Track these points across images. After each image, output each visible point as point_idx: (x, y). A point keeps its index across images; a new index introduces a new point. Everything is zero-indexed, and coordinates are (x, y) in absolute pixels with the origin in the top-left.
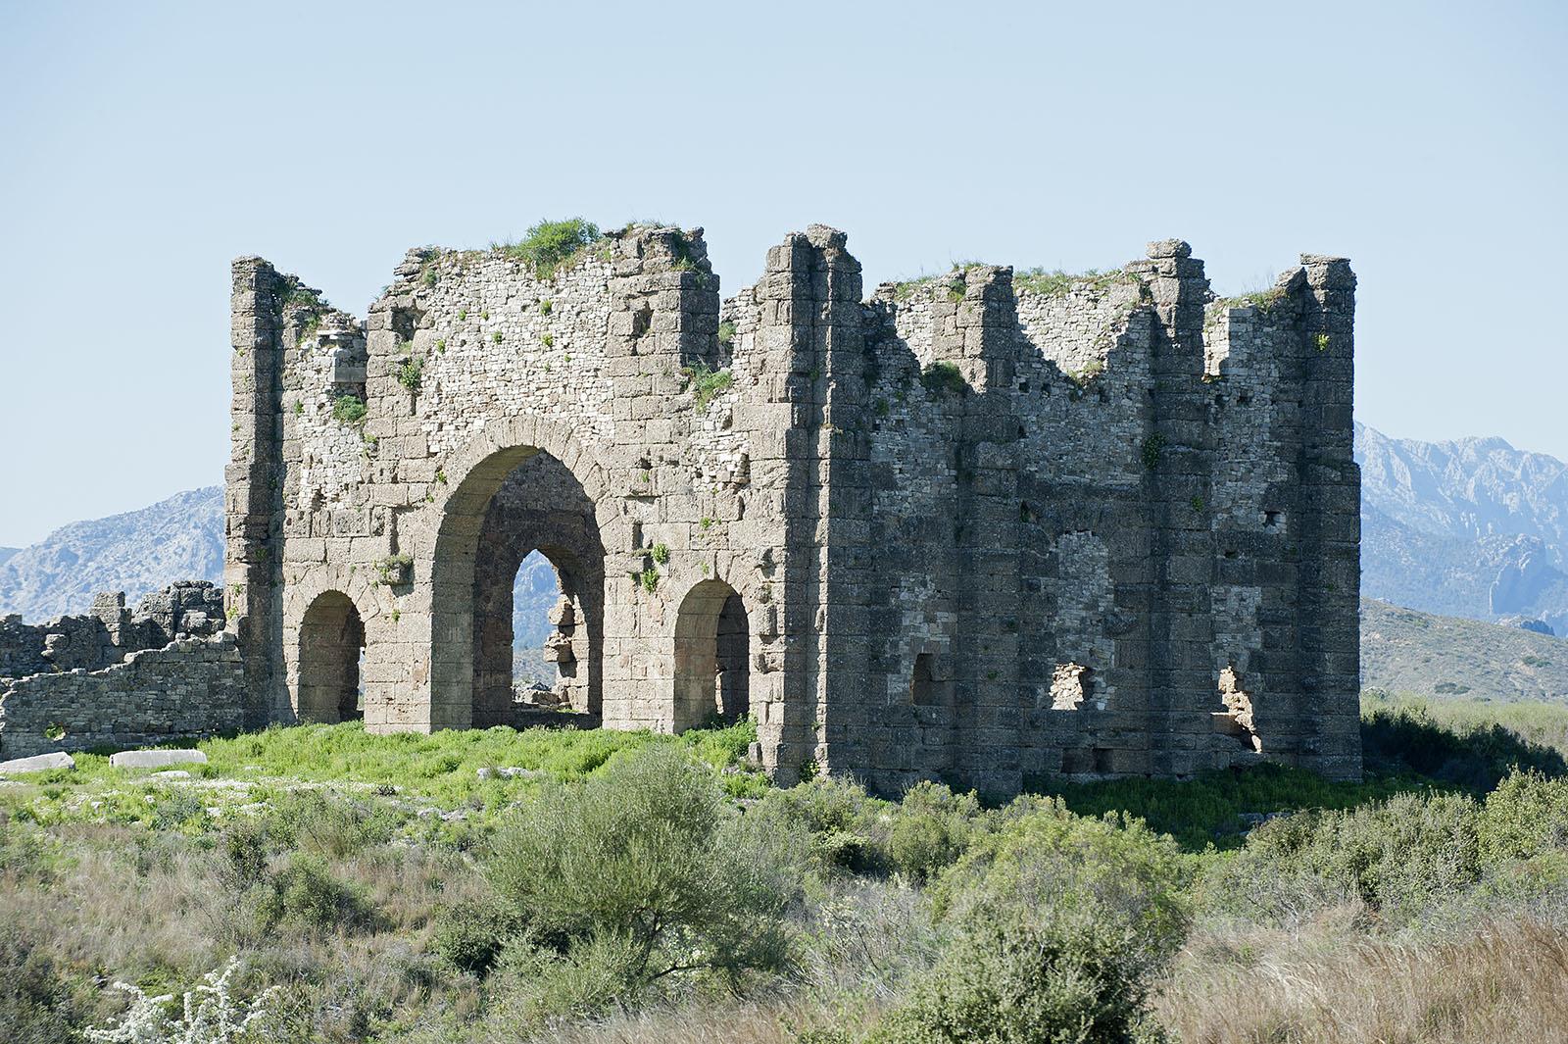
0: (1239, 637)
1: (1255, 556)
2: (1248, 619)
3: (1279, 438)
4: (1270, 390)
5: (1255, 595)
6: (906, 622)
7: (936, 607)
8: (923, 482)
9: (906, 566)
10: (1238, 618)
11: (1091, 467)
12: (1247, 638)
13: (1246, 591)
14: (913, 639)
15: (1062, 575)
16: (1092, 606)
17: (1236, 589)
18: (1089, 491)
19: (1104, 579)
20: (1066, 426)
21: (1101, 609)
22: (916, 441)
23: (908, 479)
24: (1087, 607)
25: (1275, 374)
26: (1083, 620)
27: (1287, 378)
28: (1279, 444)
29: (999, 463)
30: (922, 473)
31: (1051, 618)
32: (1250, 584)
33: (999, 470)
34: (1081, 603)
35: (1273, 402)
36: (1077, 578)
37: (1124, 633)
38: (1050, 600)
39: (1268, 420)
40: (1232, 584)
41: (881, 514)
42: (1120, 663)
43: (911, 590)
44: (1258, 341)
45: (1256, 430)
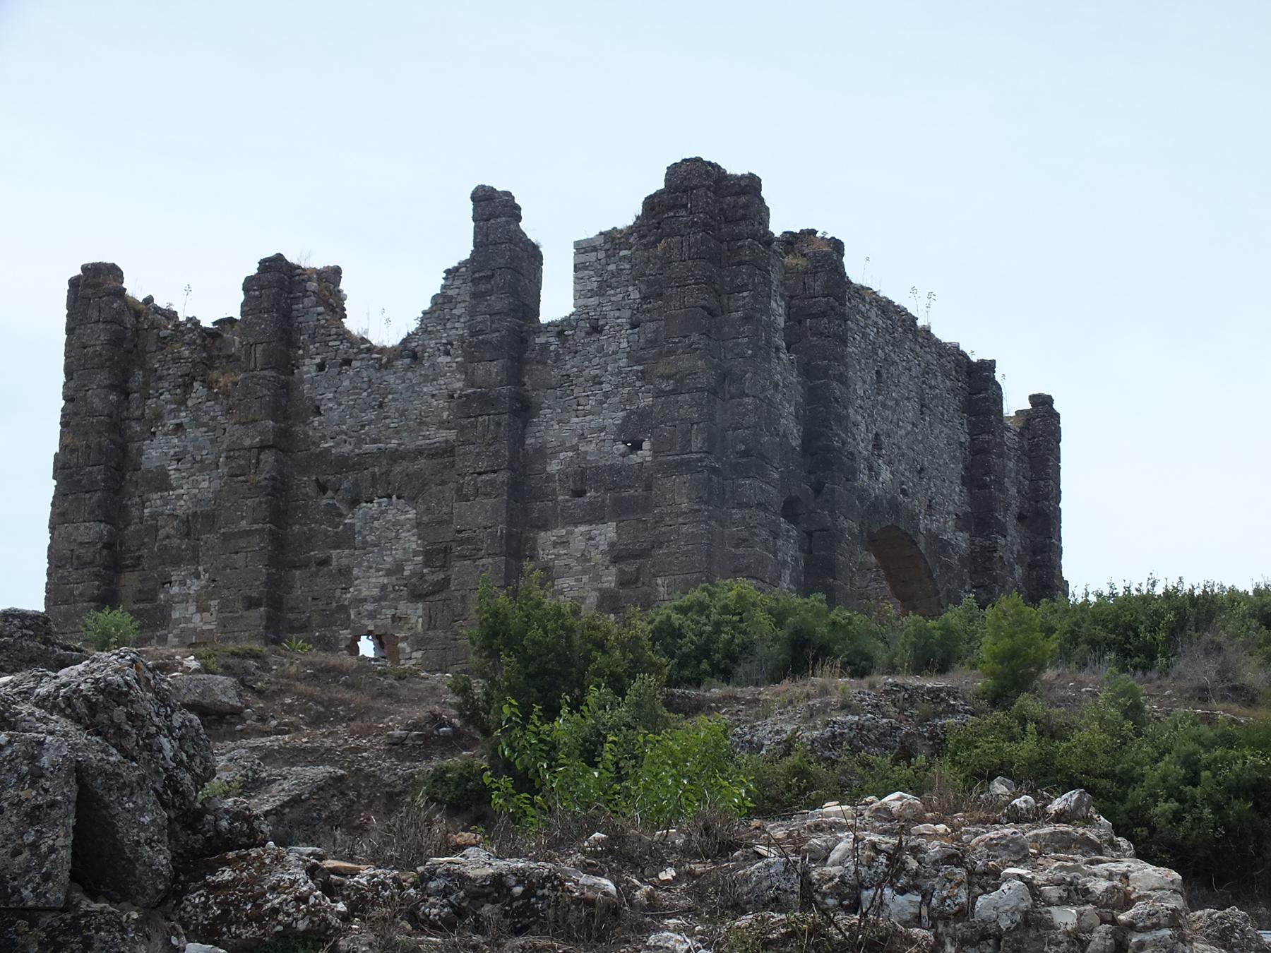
0: (585, 579)
1: (607, 490)
2: (597, 557)
3: (639, 361)
4: (627, 313)
5: (607, 532)
6: (175, 615)
8: (200, 478)
9: (176, 563)
10: (584, 558)
11: (398, 432)
12: (597, 578)
13: (595, 530)
14: (183, 630)
15: (358, 544)
16: (397, 569)
17: (582, 528)
18: (396, 456)
19: (411, 541)
20: (369, 395)
21: (406, 573)
22: (196, 439)
23: (184, 478)
24: (389, 573)
25: (635, 295)
26: (383, 587)
27: (648, 297)
28: (641, 368)
29: (247, 443)
30: (201, 471)
31: (345, 590)
32: (602, 520)
33: (249, 449)
34: (381, 570)
35: (633, 326)
36: (376, 546)
37: (433, 593)
38: (345, 574)
39: (625, 345)
40: (576, 525)
41: (153, 516)
42: (430, 624)
43: (183, 583)
44: (612, 267)
45: (609, 359)
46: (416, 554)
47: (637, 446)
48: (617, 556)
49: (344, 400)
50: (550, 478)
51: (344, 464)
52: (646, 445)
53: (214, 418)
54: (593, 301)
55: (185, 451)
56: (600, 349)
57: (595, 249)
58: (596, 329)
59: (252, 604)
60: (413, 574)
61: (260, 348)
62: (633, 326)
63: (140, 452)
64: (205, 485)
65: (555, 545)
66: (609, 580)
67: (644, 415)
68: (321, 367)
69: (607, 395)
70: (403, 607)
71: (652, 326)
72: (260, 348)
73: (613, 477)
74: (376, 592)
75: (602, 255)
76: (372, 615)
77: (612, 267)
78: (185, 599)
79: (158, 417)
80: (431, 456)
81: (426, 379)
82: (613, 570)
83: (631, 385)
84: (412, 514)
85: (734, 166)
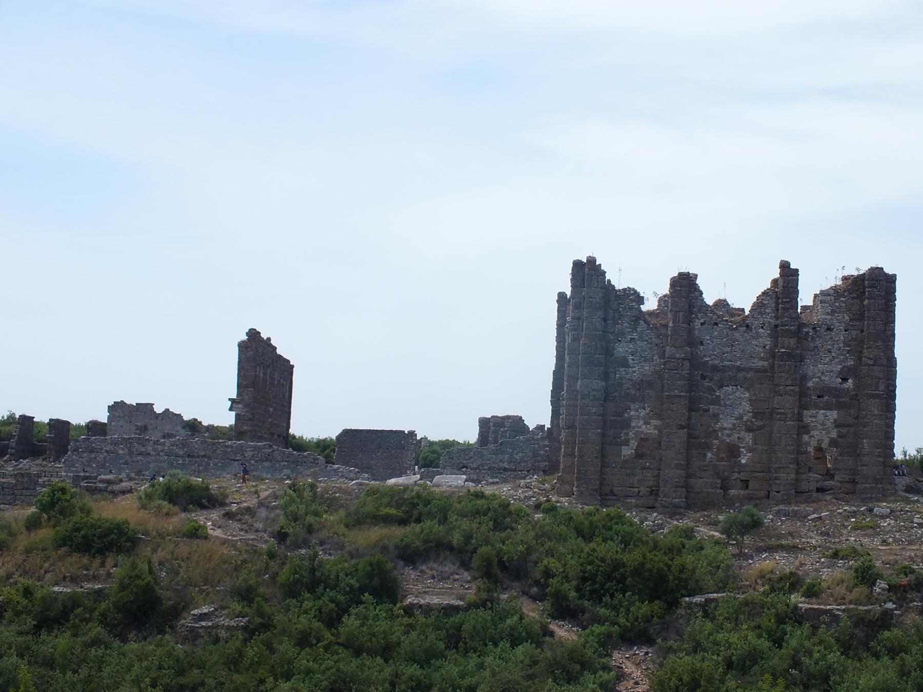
0: (824, 432)
2: (828, 424)
4: (844, 325)
5: (833, 415)
6: (633, 424)
7: (651, 418)
9: (634, 401)
10: (823, 424)
12: (829, 433)
13: (828, 413)
16: (740, 417)
17: (822, 411)
18: (739, 369)
24: (736, 419)
25: (847, 318)
26: (734, 424)
29: (678, 356)
38: (716, 416)
41: (620, 378)
42: (755, 443)
43: (637, 410)
44: (837, 304)
46: (749, 412)
47: (845, 380)
48: (837, 424)
49: (715, 340)
50: (809, 388)
51: (715, 369)
52: (850, 381)
53: (651, 338)
54: (829, 317)
55: (636, 351)
56: (831, 338)
57: (829, 295)
59: (682, 427)
60: (748, 420)
61: (681, 314)
64: (647, 368)
65: (811, 417)
66: (834, 434)
67: (849, 368)
68: (702, 324)
70: (743, 434)
71: (854, 332)
72: (681, 314)
74: (730, 426)
75: (833, 298)
76: (729, 436)
77: (837, 304)
78: (638, 418)
79: (623, 334)
81: (753, 338)
82: (835, 430)
83: (845, 355)
84: (747, 395)
85: (888, 270)
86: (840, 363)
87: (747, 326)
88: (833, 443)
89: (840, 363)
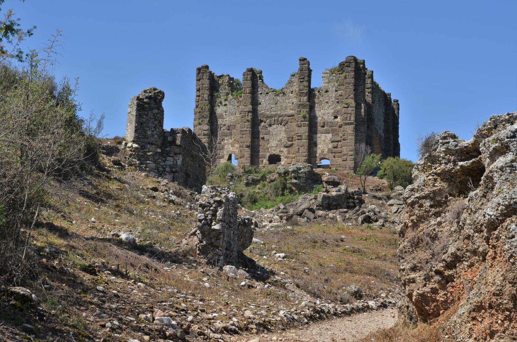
3: (337, 99)
4: (334, 88)
5: (330, 136)
6: (226, 147)
9: (226, 136)
13: (327, 135)
16: (281, 141)
24: (278, 141)
26: (277, 144)
29: (245, 110)
38: (268, 140)
43: (227, 140)
47: (336, 117)
51: (268, 117)
52: (339, 117)
54: (327, 85)
58: (327, 91)
62: (336, 91)
63: (216, 110)
66: (331, 146)
69: (330, 106)
73: (332, 125)
74: (275, 145)
76: (274, 150)
80: (289, 116)
84: (284, 129)
86: (333, 109)
87: (284, 93)
88: (330, 151)
89: (333, 109)
